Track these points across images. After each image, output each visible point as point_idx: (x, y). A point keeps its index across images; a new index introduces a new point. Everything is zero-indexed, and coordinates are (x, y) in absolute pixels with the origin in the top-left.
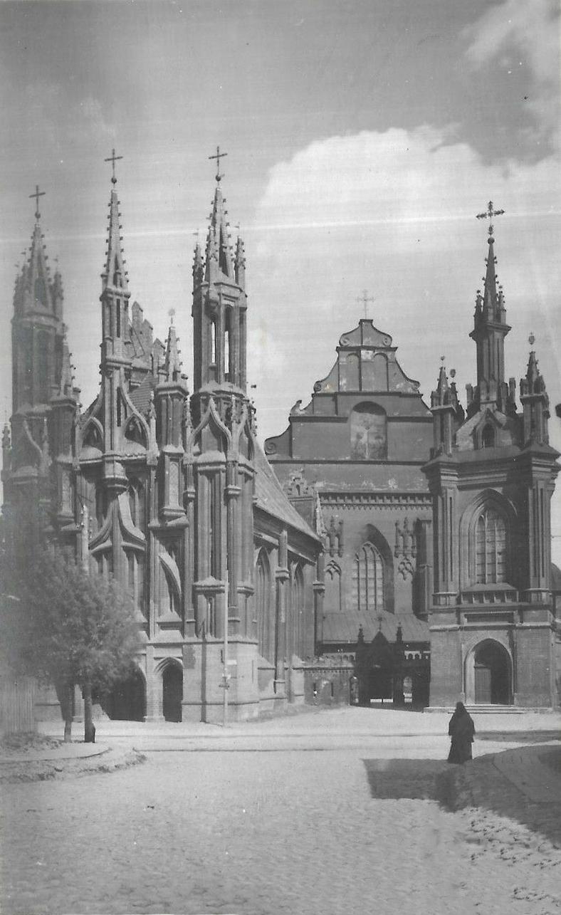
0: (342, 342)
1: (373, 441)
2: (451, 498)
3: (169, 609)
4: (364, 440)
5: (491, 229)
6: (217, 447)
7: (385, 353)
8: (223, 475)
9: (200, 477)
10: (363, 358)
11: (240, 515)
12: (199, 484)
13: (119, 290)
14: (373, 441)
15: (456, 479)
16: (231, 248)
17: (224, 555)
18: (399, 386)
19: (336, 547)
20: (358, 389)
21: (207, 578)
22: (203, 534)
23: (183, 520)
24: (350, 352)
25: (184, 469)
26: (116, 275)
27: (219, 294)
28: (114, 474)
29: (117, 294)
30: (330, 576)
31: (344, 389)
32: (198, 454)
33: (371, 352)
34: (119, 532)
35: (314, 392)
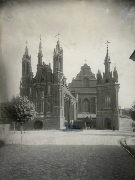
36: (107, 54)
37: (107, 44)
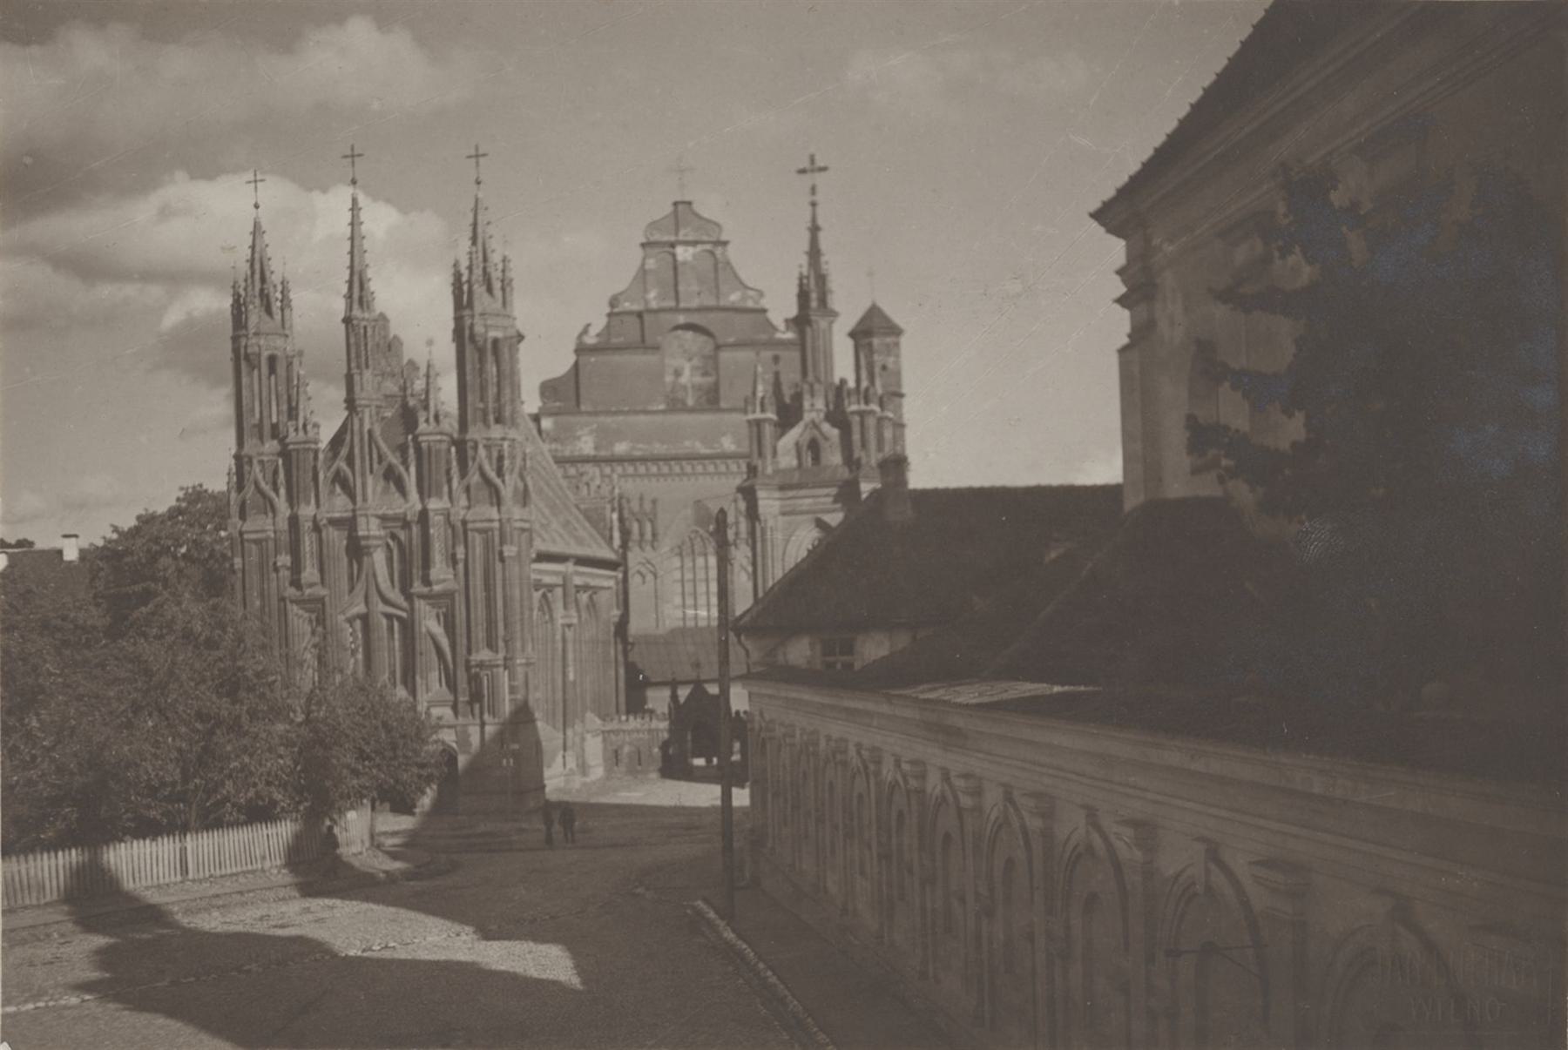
0: (649, 236)
1: (698, 379)
3: (438, 685)
4: (684, 380)
5: (813, 190)
8: (497, 533)
9: (470, 534)
10: (680, 258)
12: (470, 544)
13: (366, 315)
14: (698, 379)
16: (496, 265)
17: (501, 625)
18: (734, 298)
19: (648, 536)
23: (451, 585)
27: (486, 326)
29: (363, 319)
31: (654, 305)
32: (469, 508)
33: (691, 250)
35: (608, 310)
36: (814, 253)
37: (807, 180)
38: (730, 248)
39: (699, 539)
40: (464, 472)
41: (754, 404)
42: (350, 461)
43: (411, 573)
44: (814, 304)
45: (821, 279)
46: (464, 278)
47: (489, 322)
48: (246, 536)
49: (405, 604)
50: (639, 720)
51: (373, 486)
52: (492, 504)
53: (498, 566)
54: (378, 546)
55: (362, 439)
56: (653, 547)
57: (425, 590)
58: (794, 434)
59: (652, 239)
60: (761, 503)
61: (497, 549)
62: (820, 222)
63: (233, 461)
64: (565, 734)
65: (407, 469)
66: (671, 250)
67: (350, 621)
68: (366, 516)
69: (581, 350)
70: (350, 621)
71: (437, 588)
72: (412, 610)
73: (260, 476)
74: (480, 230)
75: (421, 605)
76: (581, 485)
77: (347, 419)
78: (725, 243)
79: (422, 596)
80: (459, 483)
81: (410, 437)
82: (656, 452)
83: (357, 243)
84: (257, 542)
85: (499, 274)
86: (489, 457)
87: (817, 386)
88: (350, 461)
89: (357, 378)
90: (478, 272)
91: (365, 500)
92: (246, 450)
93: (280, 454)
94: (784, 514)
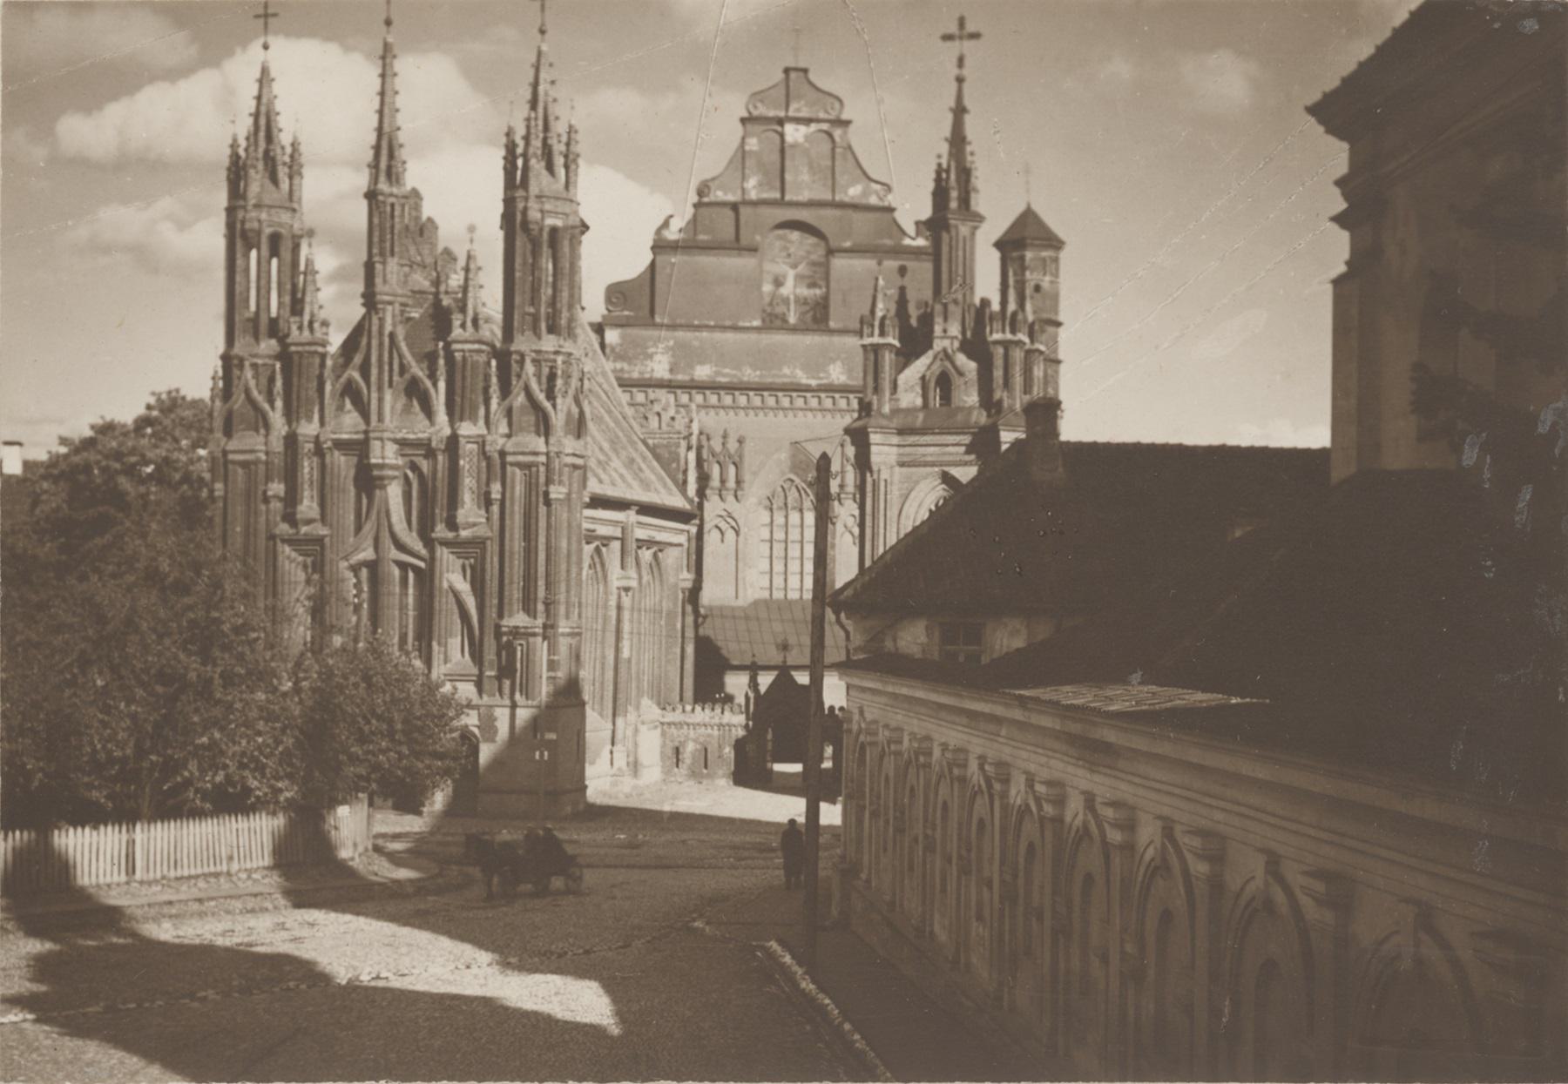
0: (752, 109)
1: (804, 292)
2: (886, 481)
3: (459, 655)
4: (787, 290)
5: (961, 62)
6: (533, 429)
7: (831, 130)
8: (542, 469)
9: (509, 468)
10: (789, 139)
11: (566, 524)
12: (508, 480)
13: (395, 190)
14: (804, 292)
15: (895, 450)
17: (541, 583)
18: (854, 192)
19: (731, 484)
20: (777, 195)
21: (516, 616)
22: (512, 553)
23: (482, 531)
24: (765, 127)
25: (483, 453)
26: (389, 168)
27: (542, 211)
28: (383, 458)
29: (391, 195)
30: (719, 536)
31: (753, 195)
32: (509, 436)
33: (803, 129)
34: (387, 534)
35: (695, 199)
36: (958, 140)
37: (954, 48)
38: (852, 128)
39: (794, 489)
40: (506, 391)
41: (872, 326)
42: (365, 370)
43: (433, 514)
44: (954, 205)
45: (965, 174)
46: (520, 150)
47: (548, 207)
48: (231, 457)
49: (424, 552)
50: (707, 711)
51: (391, 401)
52: (538, 434)
53: (543, 509)
54: (395, 478)
55: (381, 344)
56: (736, 497)
57: (451, 535)
58: (920, 366)
59: (755, 113)
60: (874, 449)
61: (542, 489)
62: (967, 102)
63: (220, 363)
64: (614, 724)
65: (435, 385)
66: (779, 129)
67: (355, 569)
68: (381, 439)
69: (660, 246)
70: (355, 569)
71: (464, 533)
72: (431, 561)
73: (252, 383)
74: (541, 88)
75: (444, 554)
76: (650, 416)
77: (364, 318)
78: (847, 123)
79: (446, 543)
80: (499, 404)
81: (441, 344)
82: (745, 379)
83: (387, 99)
84: (245, 465)
85: (563, 148)
86: (538, 375)
87: (952, 307)
88: (365, 370)
89: (379, 267)
90: (537, 143)
91: (381, 419)
92: (238, 350)
93: (278, 357)
94: (902, 464)
